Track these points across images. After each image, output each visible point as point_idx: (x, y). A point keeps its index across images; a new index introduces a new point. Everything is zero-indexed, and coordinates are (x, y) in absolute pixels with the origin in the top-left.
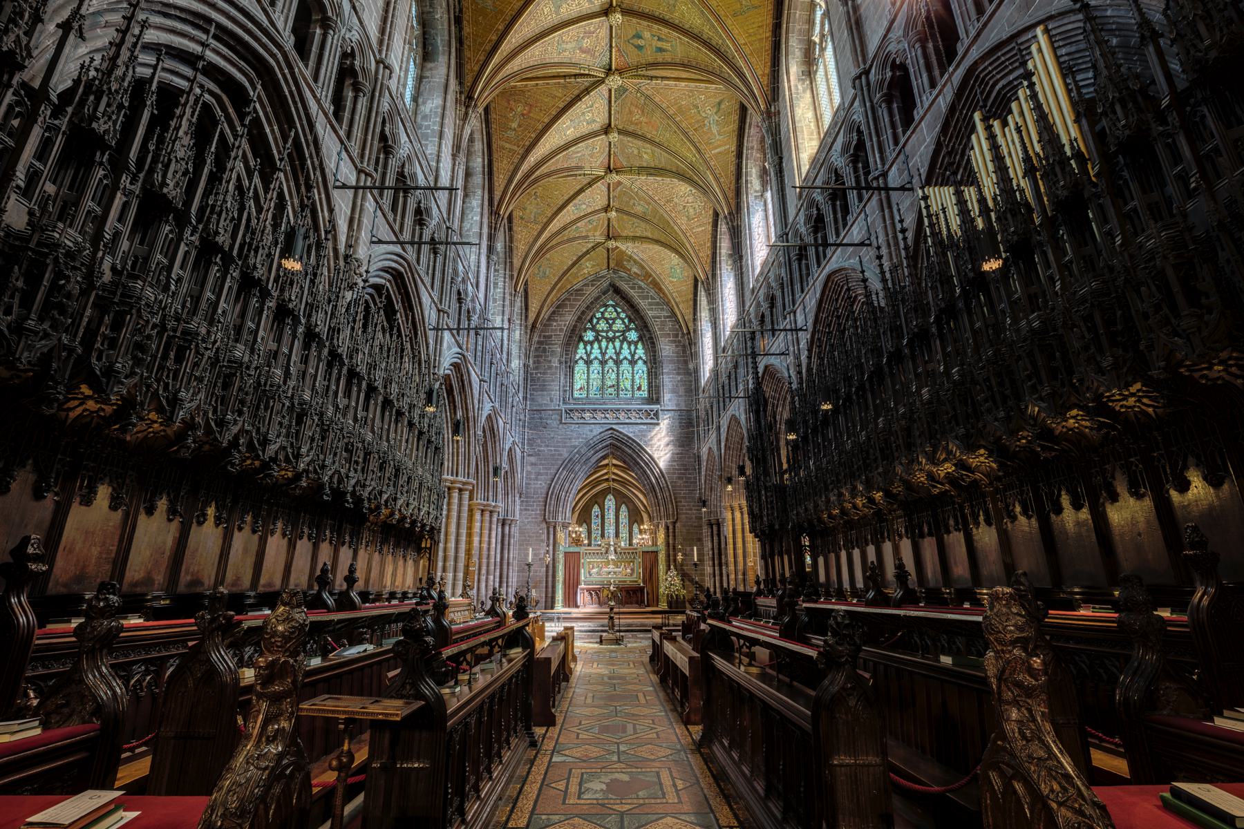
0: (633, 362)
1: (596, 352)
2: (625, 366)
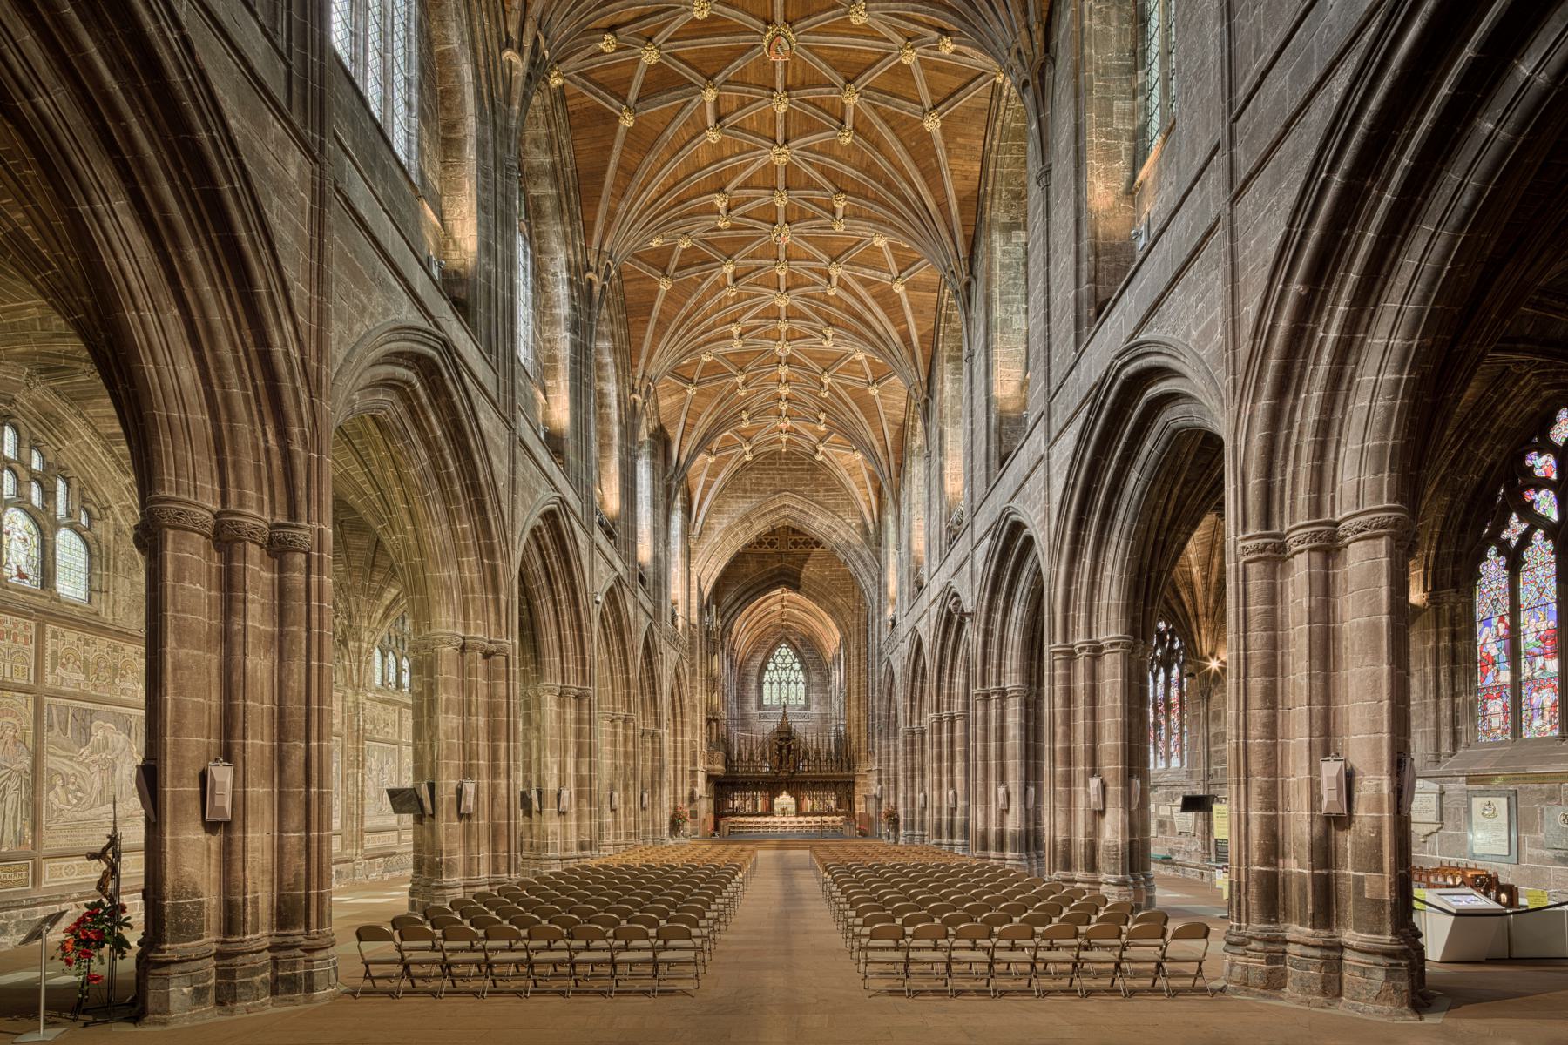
0: (797, 683)
1: (775, 677)
2: (792, 685)
